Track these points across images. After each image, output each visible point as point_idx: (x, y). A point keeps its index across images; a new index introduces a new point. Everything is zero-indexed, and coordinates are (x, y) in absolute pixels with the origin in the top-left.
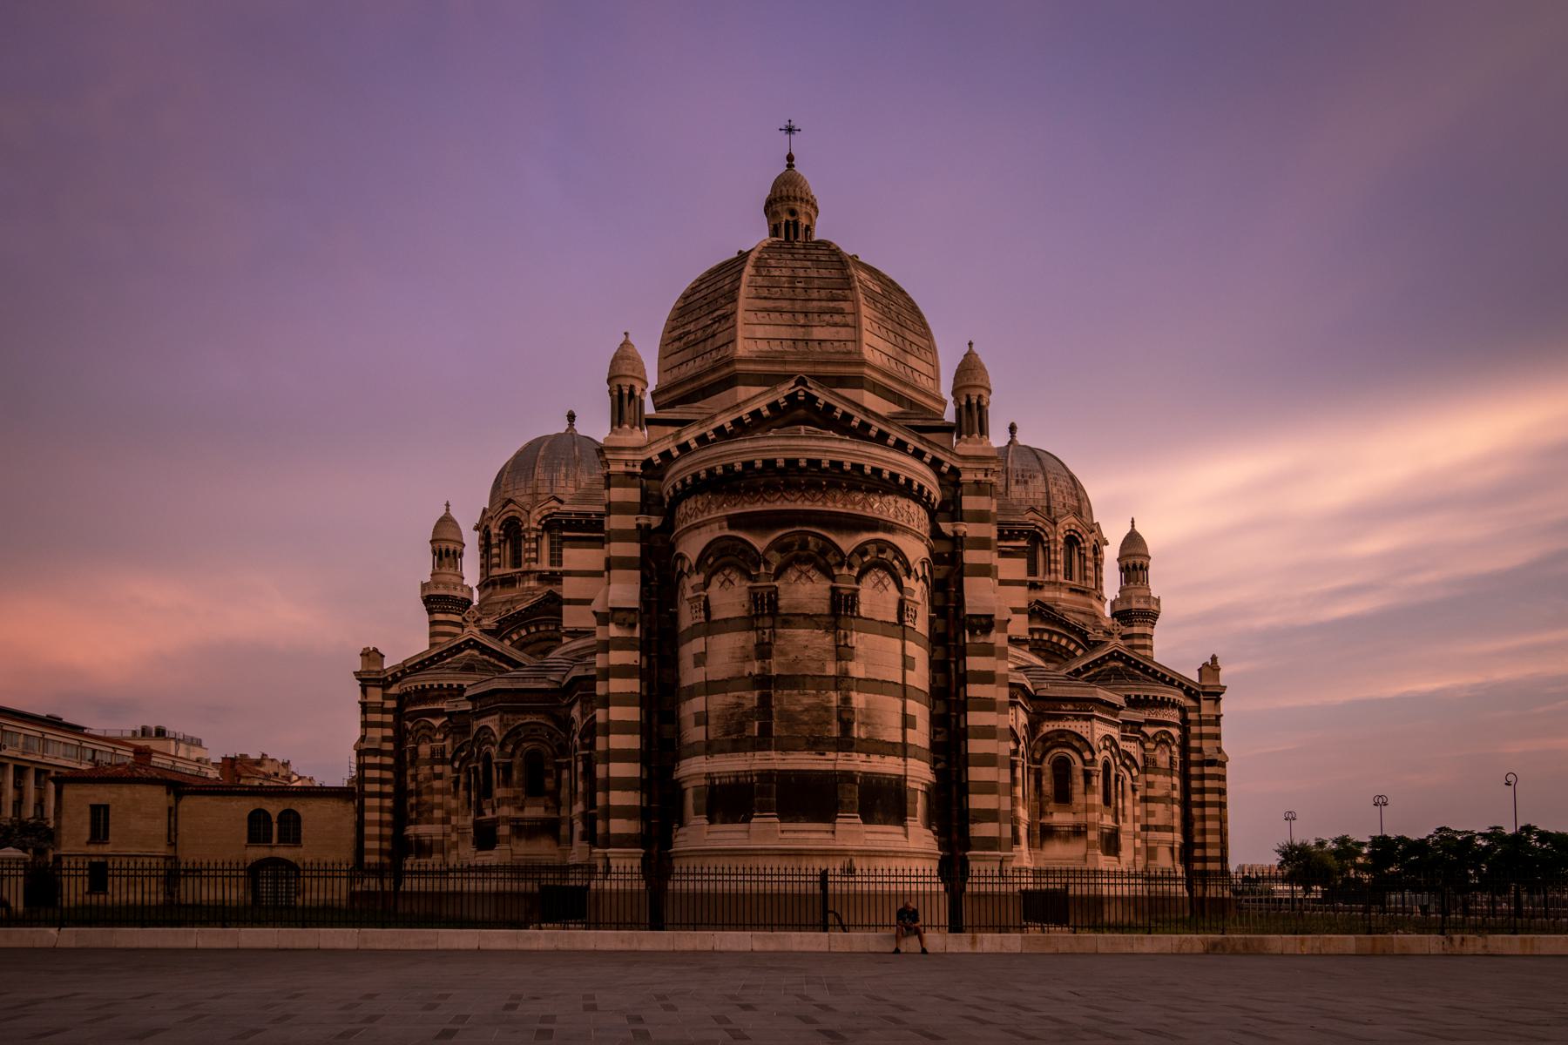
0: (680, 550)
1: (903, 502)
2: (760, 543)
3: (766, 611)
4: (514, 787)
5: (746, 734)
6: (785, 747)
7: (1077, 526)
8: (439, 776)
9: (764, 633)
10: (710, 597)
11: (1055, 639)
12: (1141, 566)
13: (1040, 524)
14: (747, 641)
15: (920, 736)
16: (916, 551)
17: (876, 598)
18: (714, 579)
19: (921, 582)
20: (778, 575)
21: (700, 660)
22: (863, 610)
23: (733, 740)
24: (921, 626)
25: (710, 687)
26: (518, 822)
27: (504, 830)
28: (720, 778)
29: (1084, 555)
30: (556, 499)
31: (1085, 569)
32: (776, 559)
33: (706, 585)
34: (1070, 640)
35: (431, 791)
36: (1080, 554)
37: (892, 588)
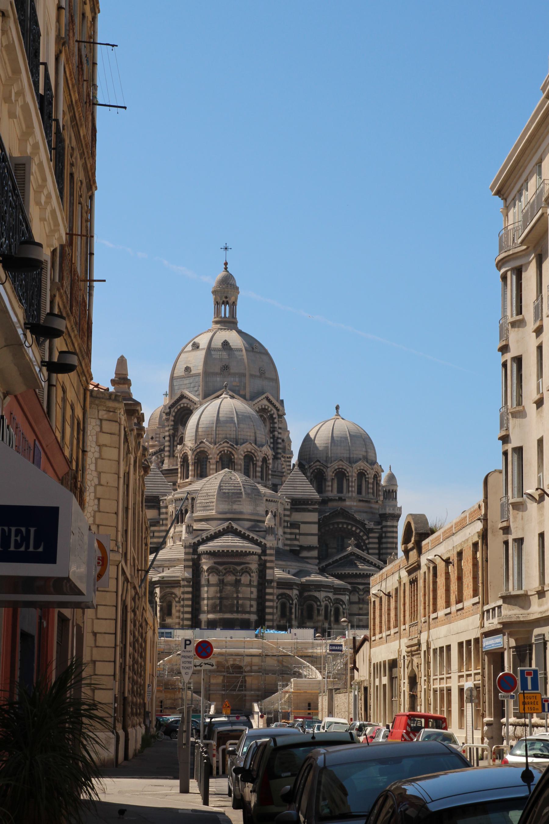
1: (251, 557)
7: (364, 467)
11: (350, 527)
12: (393, 490)
13: (345, 467)
15: (254, 609)
16: (254, 567)
17: (245, 579)
19: (256, 573)
20: (225, 574)
22: (242, 582)
24: (255, 583)
29: (368, 481)
31: (368, 488)
32: (224, 571)
34: (357, 528)
36: (366, 481)
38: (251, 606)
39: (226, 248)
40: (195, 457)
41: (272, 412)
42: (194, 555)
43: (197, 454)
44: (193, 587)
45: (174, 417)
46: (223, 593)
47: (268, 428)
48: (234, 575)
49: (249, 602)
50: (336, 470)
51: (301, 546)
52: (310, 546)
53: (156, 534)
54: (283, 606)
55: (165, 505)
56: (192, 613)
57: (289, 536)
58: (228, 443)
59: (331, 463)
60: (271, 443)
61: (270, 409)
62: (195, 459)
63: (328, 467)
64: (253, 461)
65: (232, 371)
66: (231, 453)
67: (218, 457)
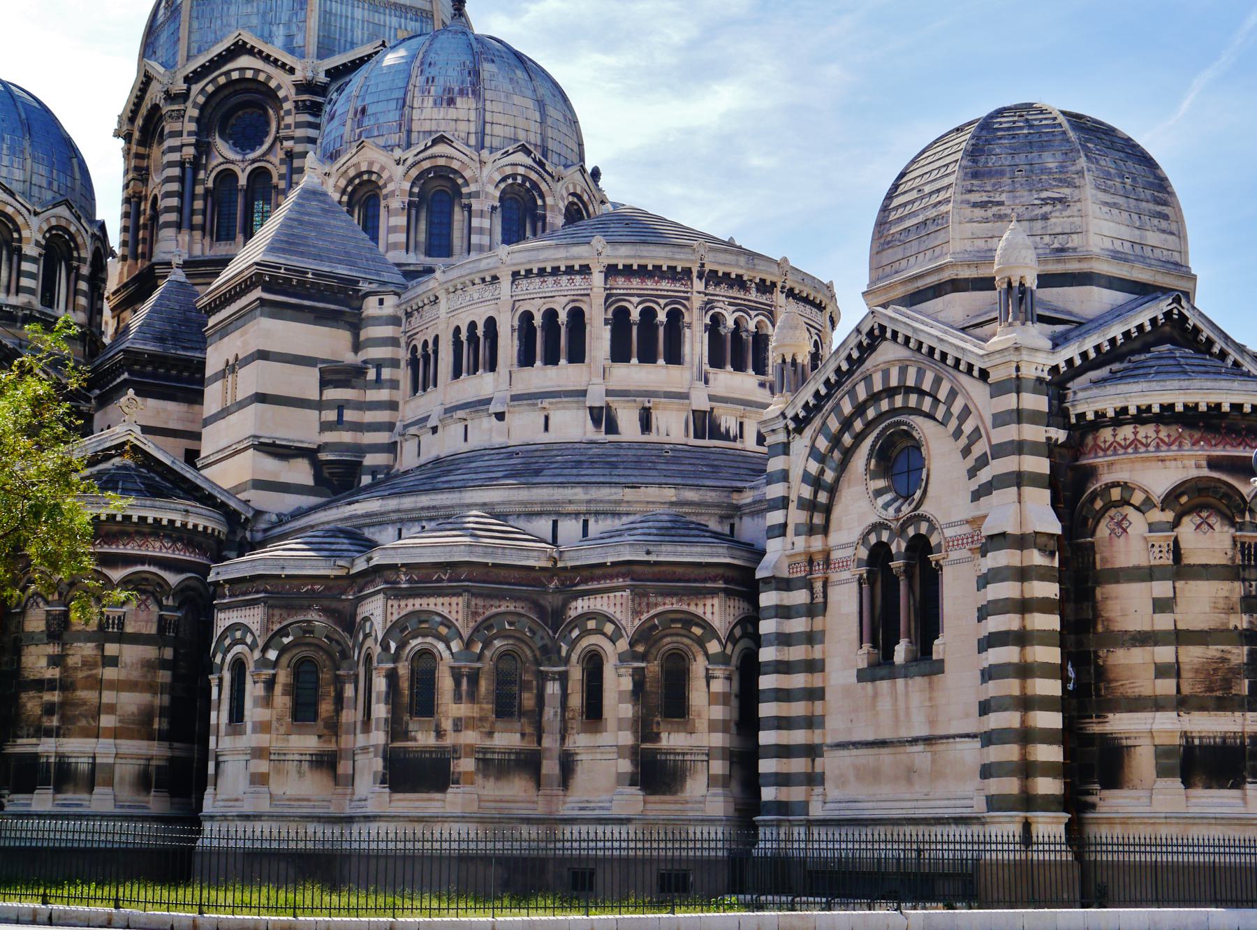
3: (1253, 563)
4: (478, 703)
5: (1234, 692)
8: (113, 661)
9: (1251, 586)
10: (1179, 539)
14: (1232, 591)
18: (1186, 520)
23: (1218, 698)
26: (484, 753)
27: (466, 765)
28: (1200, 738)
33: (1176, 523)
35: (99, 684)
40: (412, 187)
43: (418, 178)
44: (1060, 576)
53: (349, 415)
58: (528, 153)
62: (411, 194)
66: (535, 185)
67: (497, 194)
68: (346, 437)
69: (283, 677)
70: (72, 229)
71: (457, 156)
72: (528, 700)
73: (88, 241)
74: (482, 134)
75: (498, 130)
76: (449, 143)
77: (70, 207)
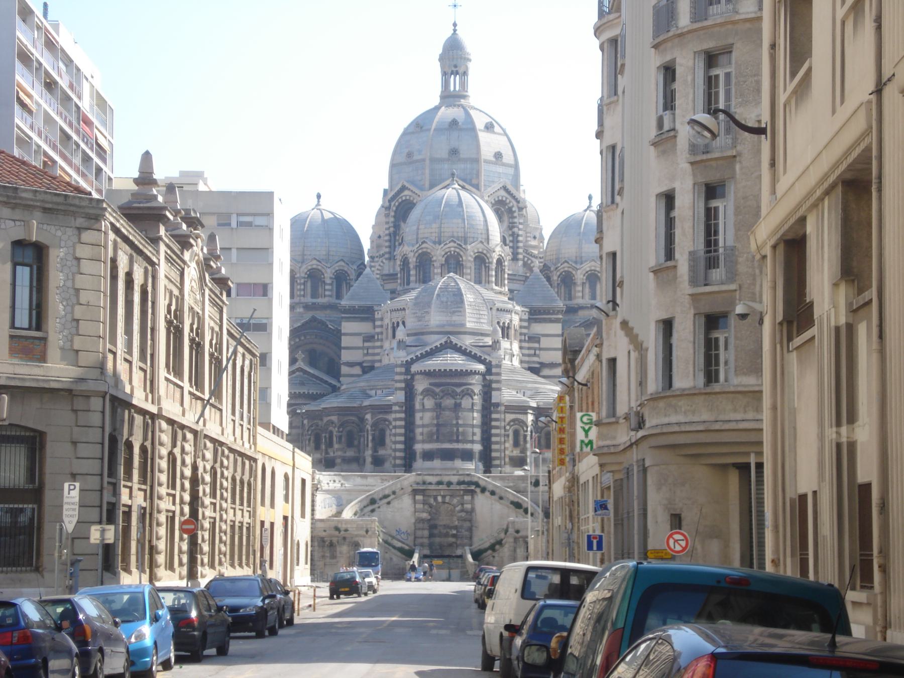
0: (416, 387)
2: (437, 390)
6: (443, 442)
15: (478, 437)
16: (477, 389)
17: (466, 403)
20: (442, 398)
21: (422, 418)
22: (463, 406)
25: (423, 426)
30: (315, 259)
32: (441, 394)
37: (470, 400)
38: (474, 434)
39: (455, 6)
41: (511, 204)
42: (407, 375)
44: (405, 412)
45: (395, 212)
46: (441, 419)
47: (506, 224)
48: (453, 397)
49: (471, 429)
50: (587, 272)
51: (541, 363)
52: (552, 363)
53: (370, 351)
54: (516, 433)
55: (380, 316)
56: (405, 443)
57: (526, 352)
58: (455, 242)
59: (582, 263)
60: (510, 241)
61: (508, 201)
62: (416, 262)
63: (577, 269)
64: (485, 263)
65: (461, 156)
66: (458, 254)
67: (444, 259)
68: (369, 358)
69: (312, 438)
70: (346, 269)
71: (428, 246)
72: (356, 442)
73: (353, 271)
74: (440, 237)
75: (446, 234)
76: (426, 243)
77: (344, 261)
